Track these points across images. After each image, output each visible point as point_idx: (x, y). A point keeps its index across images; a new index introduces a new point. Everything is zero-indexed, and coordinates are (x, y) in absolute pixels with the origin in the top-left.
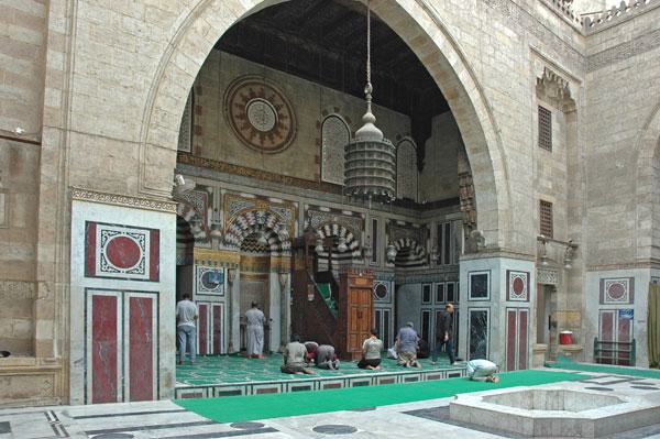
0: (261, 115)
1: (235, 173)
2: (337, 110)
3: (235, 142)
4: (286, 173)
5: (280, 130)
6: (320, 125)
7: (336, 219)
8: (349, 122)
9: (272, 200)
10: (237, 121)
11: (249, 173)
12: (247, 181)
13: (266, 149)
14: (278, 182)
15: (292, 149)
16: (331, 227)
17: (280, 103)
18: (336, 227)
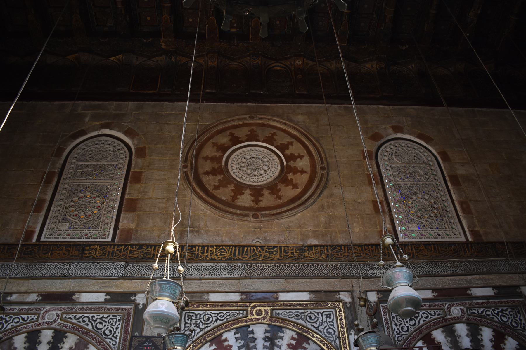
0: (255, 164)
2: (397, 129)
4: (313, 242)
5: (290, 176)
6: (374, 156)
7: (456, 311)
8: (428, 140)
9: (283, 297)
10: (205, 179)
11: (228, 255)
12: (223, 269)
13: (266, 209)
14: (297, 260)
15: (323, 200)
16: (450, 332)
17: (287, 139)
18: (461, 329)
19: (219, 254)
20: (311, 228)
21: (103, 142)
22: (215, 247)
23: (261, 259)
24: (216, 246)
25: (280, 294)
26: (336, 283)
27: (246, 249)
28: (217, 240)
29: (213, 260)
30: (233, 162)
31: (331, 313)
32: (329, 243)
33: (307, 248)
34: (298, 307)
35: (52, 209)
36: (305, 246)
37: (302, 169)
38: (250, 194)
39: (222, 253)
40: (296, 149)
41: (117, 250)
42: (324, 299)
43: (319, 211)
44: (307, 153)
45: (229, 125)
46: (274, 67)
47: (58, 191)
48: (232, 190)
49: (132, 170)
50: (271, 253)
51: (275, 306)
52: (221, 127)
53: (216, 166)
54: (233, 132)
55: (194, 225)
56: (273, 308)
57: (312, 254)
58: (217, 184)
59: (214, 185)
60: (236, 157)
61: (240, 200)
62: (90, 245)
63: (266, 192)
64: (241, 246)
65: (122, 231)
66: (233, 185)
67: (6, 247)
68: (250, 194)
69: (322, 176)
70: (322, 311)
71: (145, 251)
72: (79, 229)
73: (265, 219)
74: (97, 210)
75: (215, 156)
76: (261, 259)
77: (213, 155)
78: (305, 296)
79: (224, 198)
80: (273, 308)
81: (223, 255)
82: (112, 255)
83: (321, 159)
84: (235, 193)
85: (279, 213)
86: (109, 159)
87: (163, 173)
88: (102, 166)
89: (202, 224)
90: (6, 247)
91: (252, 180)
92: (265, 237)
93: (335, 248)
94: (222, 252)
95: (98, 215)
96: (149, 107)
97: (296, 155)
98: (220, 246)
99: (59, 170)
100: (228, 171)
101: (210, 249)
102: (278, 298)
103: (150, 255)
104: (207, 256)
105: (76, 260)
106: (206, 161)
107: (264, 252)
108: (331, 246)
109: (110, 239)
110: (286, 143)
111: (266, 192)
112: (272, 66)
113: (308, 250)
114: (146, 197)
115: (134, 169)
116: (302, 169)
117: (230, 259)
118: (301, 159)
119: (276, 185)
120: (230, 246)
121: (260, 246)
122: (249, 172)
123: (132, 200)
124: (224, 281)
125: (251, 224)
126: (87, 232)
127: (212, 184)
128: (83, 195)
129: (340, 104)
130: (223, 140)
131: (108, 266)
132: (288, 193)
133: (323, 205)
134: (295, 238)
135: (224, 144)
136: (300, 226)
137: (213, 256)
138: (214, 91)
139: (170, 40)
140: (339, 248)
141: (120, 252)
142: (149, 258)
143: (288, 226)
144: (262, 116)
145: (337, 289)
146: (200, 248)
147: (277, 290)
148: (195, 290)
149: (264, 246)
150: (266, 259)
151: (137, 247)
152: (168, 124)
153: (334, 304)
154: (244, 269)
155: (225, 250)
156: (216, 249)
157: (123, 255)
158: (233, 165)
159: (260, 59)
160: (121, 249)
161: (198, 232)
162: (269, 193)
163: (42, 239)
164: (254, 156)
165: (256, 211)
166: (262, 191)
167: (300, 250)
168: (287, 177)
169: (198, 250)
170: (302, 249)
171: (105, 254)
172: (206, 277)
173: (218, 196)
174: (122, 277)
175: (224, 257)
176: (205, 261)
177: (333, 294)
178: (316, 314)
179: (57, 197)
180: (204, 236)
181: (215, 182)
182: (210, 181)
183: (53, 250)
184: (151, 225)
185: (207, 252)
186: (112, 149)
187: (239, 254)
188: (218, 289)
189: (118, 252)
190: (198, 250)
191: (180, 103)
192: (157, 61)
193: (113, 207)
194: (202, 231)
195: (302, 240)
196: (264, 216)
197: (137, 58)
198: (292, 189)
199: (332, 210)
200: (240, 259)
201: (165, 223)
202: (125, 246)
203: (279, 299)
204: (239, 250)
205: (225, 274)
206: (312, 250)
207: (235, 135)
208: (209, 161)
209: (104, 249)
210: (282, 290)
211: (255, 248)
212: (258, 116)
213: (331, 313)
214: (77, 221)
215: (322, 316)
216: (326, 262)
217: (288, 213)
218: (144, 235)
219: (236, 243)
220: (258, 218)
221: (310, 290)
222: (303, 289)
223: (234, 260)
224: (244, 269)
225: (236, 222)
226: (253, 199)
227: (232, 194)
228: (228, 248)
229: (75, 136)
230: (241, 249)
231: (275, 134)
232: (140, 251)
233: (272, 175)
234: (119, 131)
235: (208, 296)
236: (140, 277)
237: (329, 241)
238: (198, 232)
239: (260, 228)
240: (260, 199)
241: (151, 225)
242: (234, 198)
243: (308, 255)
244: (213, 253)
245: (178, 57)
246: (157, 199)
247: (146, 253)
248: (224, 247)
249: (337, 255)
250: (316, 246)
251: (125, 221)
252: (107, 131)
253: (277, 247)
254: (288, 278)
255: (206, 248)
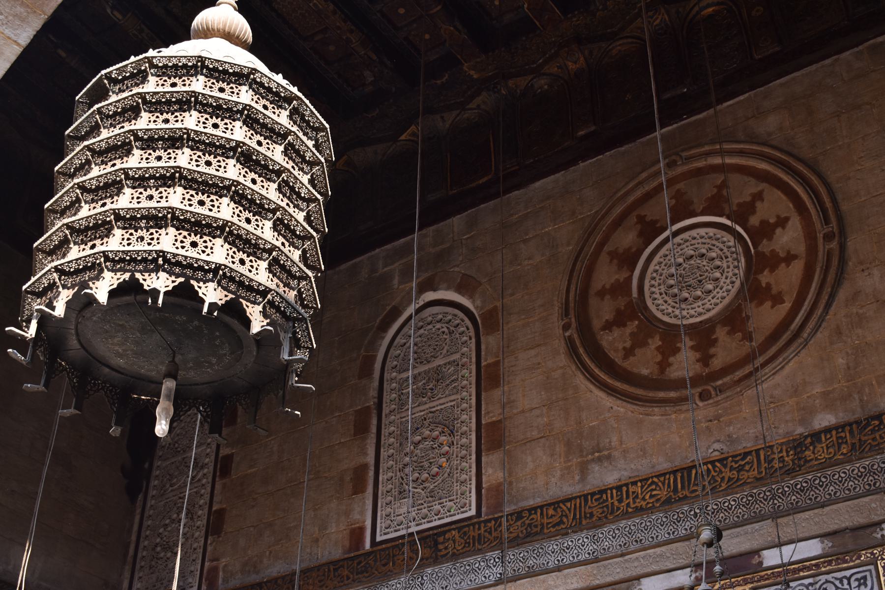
0: (692, 270)
1: (611, 515)
3: (602, 405)
4: (825, 420)
9: (771, 558)
11: (663, 494)
12: (657, 526)
14: (791, 472)
15: (838, 313)
19: (647, 497)
20: (818, 389)
21: (430, 319)
22: (639, 484)
23: (724, 486)
24: (641, 481)
25: (765, 553)
26: (873, 505)
27: (694, 472)
28: (643, 467)
29: (639, 511)
30: (653, 282)
31: (868, 574)
32: (859, 414)
33: (809, 440)
34: (802, 574)
35: (380, 479)
36: (806, 437)
37: (788, 252)
38: (692, 348)
39: (654, 493)
40: (773, 205)
41: (485, 531)
42: (850, 547)
43: (832, 343)
44: (795, 207)
45: (631, 199)
46: (698, 13)
47: (382, 443)
48: (658, 349)
49: (483, 363)
50: (740, 469)
51: (759, 581)
52: (618, 210)
53: (622, 303)
54: (643, 214)
55: (601, 446)
56: (755, 584)
57: (822, 452)
58: (628, 344)
59: (624, 348)
60: (657, 267)
61: (675, 366)
62: (445, 533)
63: (721, 333)
64: (685, 469)
65: (488, 490)
66: (657, 337)
67: (332, 568)
68: (692, 348)
69: (829, 254)
70: (848, 573)
71: (527, 522)
72: (425, 505)
73: (723, 396)
74: (444, 460)
75: (617, 280)
76: (724, 486)
77: (612, 281)
78: (812, 548)
79: (645, 372)
80: (755, 584)
81: (655, 495)
82: (479, 543)
83: (824, 211)
84: (663, 354)
85: (750, 374)
86: (445, 351)
87: (533, 352)
88: (438, 370)
89: (615, 439)
90: (332, 568)
91: (692, 312)
92: (729, 436)
93: (868, 424)
94: (653, 490)
95: (448, 470)
96: (488, 213)
97: (772, 220)
98: (647, 479)
99: (376, 400)
100: (646, 308)
101: (632, 489)
102: (761, 563)
103: (536, 526)
104: (628, 505)
105: (429, 566)
106: (602, 299)
107: (728, 469)
108: (858, 422)
109: (473, 512)
110: (748, 199)
111: (721, 333)
112: (691, 16)
113: (812, 443)
114: (515, 411)
115: (486, 360)
116: (788, 252)
117: (668, 502)
118: (784, 228)
119: (739, 309)
120: (664, 474)
121: (718, 461)
122: (685, 294)
123: (494, 423)
124: (663, 549)
125: (700, 414)
126: (438, 507)
127: (620, 347)
128: (419, 438)
129: (857, 46)
130: (626, 238)
131: (477, 565)
132: (765, 318)
133: (838, 327)
134: (787, 421)
135: (630, 248)
136: (796, 391)
137: (640, 503)
138: (593, 128)
139: (478, 60)
140: (877, 422)
141: (490, 533)
142: (536, 533)
143: (772, 397)
144: (693, 152)
145: (877, 519)
146: (614, 491)
147: (759, 547)
148: (617, 578)
149: (726, 459)
150: (734, 485)
151: (514, 518)
152: (525, 241)
153: (872, 553)
154: (696, 514)
155: (657, 485)
156: (642, 487)
157: (496, 538)
158: (653, 289)
159: (663, 11)
160: (491, 528)
161: (609, 457)
162: (729, 333)
163: (379, 538)
164: (692, 252)
165: (707, 384)
166: (714, 332)
167: (795, 448)
168: (759, 282)
169: (612, 497)
170: (800, 445)
171: (469, 543)
172: (632, 548)
173: (635, 370)
174: (500, 579)
175: (658, 500)
176: (626, 515)
177: (868, 531)
178: (837, 583)
179: (384, 454)
180: (621, 463)
181: (625, 342)
182: (614, 342)
183: (394, 556)
184: (531, 465)
185: (628, 497)
186: (445, 329)
187: (683, 487)
188: (655, 568)
189: (487, 534)
190: (612, 497)
191: (538, 184)
192: (478, 106)
193: (467, 447)
194: (616, 454)
195: (803, 422)
196: (721, 390)
197: (442, 117)
198: (772, 307)
199: (860, 331)
200: (686, 497)
201: (552, 455)
202: (496, 519)
203: (765, 565)
204: (682, 477)
205: (663, 536)
206: (820, 441)
207: (648, 219)
208: (608, 297)
209: (465, 534)
210: (767, 544)
211: (710, 466)
212: (684, 154)
213: (868, 574)
214: (420, 490)
215: (849, 584)
216: (850, 461)
217: (767, 370)
218: (524, 489)
219: (678, 463)
220: (710, 398)
221: (821, 532)
222: (807, 535)
223: (676, 501)
224: (696, 514)
225: (673, 416)
226: (698, 355)
227: (659, 358)
228: (662, 479)
229: (384, 326)
230: (685, 474)
231: (724, 185)
232: (519, 523)
233: (730, 287)
234: (448, 289)
235: (639, 584)
236: (528, 572)
237: (859, 410)
238: (609, 457)
239: (717, 418)
240: (712, 351)
241: (531, 465)
242: (663, 365)
243: (812, 456)
244: (637, 497)
245: (511, 83)
246: (532, 409)
247: (530, 525)
248: (655, 480)
249: (874, 439)
250: (828, 430)
251: (490, 471)
252: (430, 296)
253: (750, 453)
254: (776, 515)
255: (624, 489)
